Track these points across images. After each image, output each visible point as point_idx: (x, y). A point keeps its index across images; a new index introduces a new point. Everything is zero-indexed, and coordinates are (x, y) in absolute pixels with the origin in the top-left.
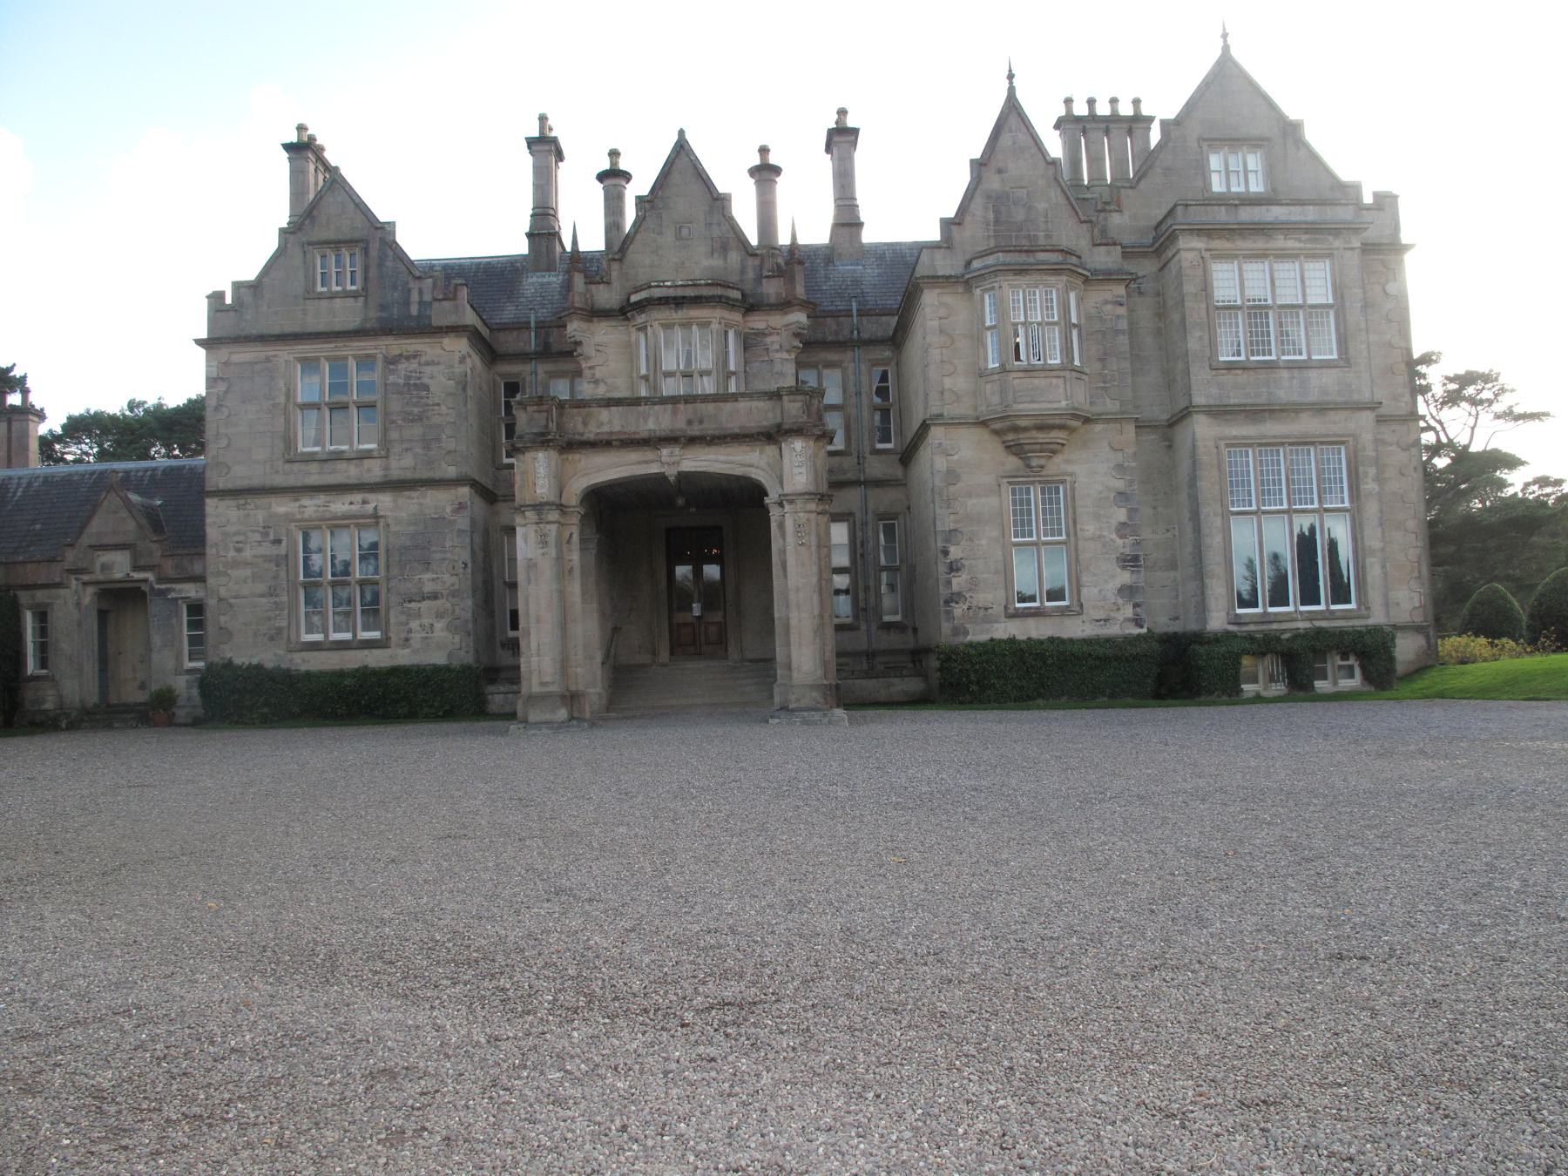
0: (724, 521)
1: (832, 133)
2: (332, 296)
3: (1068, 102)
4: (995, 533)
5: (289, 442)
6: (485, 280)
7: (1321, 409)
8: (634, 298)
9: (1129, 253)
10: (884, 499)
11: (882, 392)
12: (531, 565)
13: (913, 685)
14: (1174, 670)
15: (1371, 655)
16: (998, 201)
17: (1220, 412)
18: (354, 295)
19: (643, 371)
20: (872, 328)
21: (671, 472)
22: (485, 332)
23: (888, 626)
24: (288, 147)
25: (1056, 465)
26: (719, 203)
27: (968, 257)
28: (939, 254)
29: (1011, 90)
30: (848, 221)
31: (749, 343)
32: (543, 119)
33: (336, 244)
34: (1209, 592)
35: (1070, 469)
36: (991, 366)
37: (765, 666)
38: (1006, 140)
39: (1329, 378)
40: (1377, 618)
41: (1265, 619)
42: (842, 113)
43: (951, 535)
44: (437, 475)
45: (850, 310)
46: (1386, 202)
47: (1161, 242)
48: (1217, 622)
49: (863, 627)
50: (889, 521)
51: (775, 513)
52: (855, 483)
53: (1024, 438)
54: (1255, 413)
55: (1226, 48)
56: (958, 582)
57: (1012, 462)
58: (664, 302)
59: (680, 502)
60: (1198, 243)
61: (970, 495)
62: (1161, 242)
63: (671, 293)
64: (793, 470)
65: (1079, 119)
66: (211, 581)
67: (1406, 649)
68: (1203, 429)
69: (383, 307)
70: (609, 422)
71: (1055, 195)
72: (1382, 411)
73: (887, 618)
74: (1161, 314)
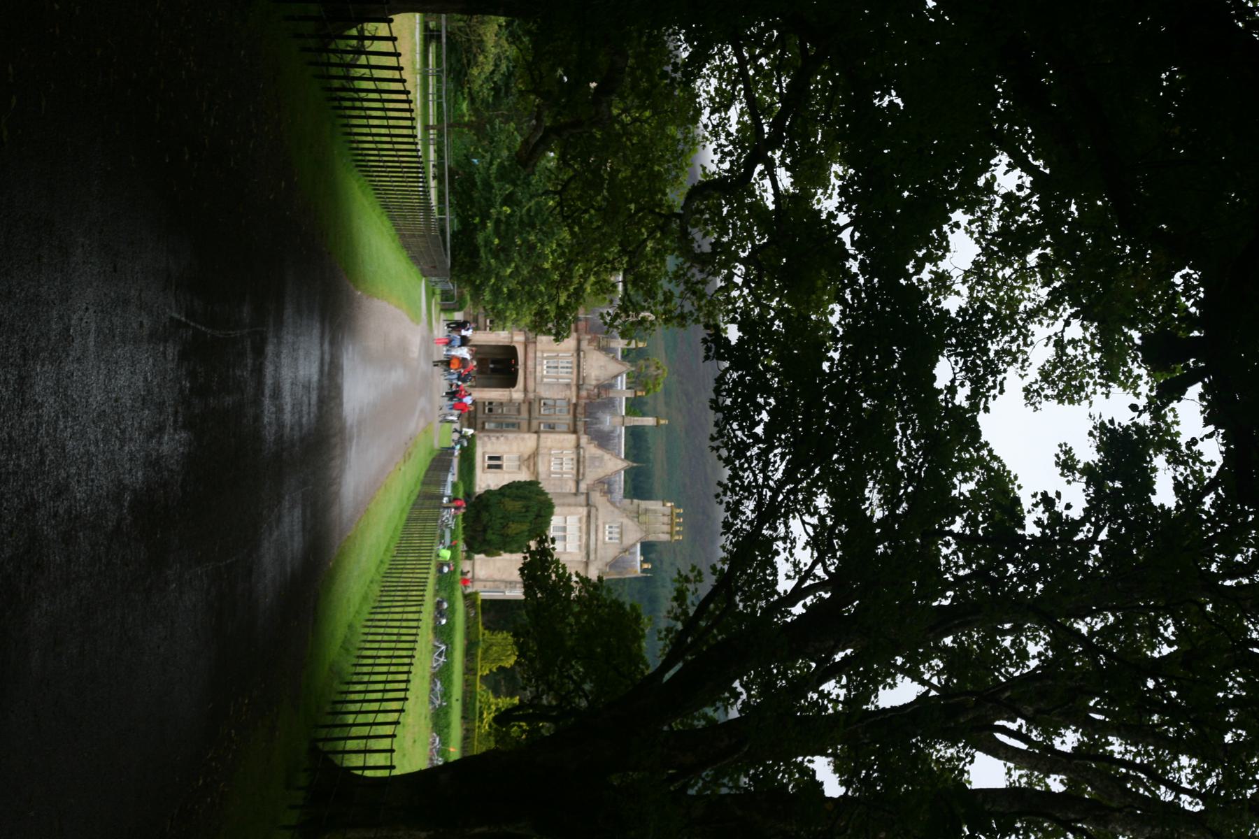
10: (524, 425)
16: (601, 459)
31: (568, 385)
43: (507, 438)
56: (494, 439)
57: (526, 456)
58: (579, 361)
64: (517, 394)
70: (531, 355)
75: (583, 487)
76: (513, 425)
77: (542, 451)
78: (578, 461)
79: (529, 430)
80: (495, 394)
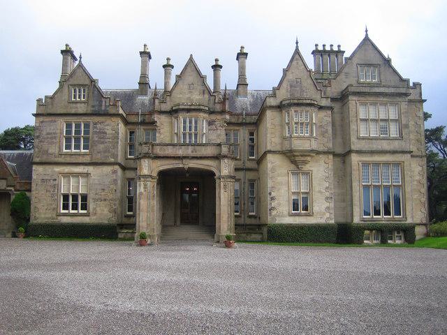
0: (204, 182)
1: (239, 54)
2: (77, 103)
3: (316, 45)
4: (287, 189)
5: (60, 149)
6: (128, 97)
7: (394, 152)
8: (174, 108)
9: (333, 100)
10: (250, 175)
11: (252, 140)
12: (141, 194)
13: (258, 237)
14: (344, 235)
15: (407, 233)
17: (359, 152)
18: (84, 103)
19: (176, 132)
20: (248, 120)
21: (186, 167)
22: (125, 115)
23: (250, 217)
24: (62, 52)
25: (306, 168)
26: (203, 78)
27: (281, 100)
28: (272, 99)
29: (297, 47)
30: (242, 83)
31: (210, 123)
32: (145, 46)
33: (79, 85)
34: (354, 210)
35: (311, 169)
36: (287, 135)
37: (209, 227)
38: (294, 63)
39: (396, 143)
40: (409, 221)
41: (372, 220)
42: (242, 48)
44: (108, 161)
45: (243, 118)
46: (417, 86)
47: (343, 98)
48: (356, 220)
49: (243, 216)
50: (252, 183)
51: (217, 181)
52: (242, 169)
53: (297, 159)
54: (372, 152)
55: (367, 35)
57: (293, 167)
58: (183, 110)
59: (187, 175)
60: (354, 98)
61: (278, 176)
62: (343, 98)
63: (186, 107)
64: (226, 168)
65: (320, 51)
66: (33, 193)
67: (419, 232)
68: (355, 158)
69: (93, 106)
70: (170, 151)
71: (309, 81)
72: (413, 154)
73: (250, 214)
74: (343, 119)
75: (324, 103)
76: (252, 185)
77: (287, 146)
78: (298, 105)
79: (256, 170)
80: (224, 199)
